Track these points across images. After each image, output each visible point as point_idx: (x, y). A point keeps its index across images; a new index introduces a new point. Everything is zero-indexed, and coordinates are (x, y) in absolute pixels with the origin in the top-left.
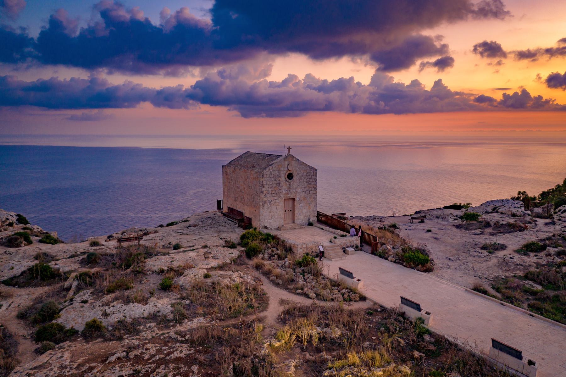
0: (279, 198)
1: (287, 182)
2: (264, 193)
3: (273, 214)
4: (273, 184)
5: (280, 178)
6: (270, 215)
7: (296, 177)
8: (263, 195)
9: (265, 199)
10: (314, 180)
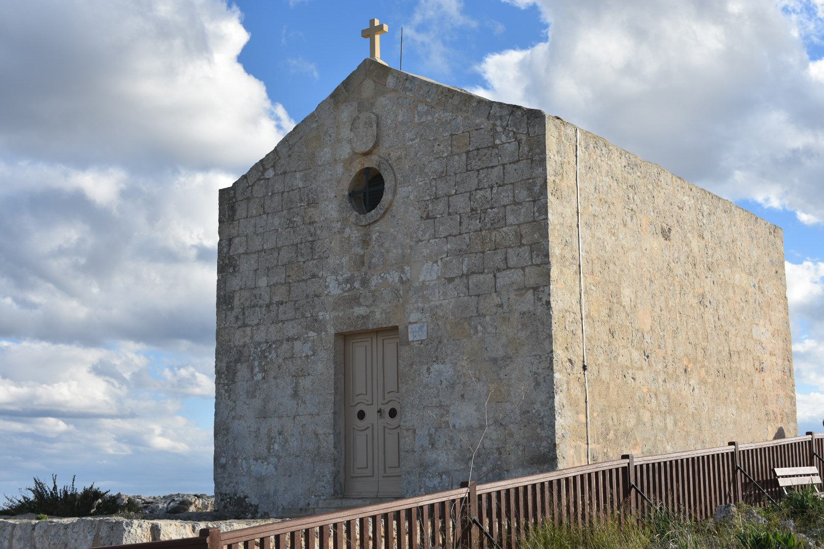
0: (308, 328)
2: (236, 302)
3: (275, 424)
4: (279, 249)
5: (311, 211)
6: (264, 431)
8: (231, 317)
9: (239, 338)
10: (523, 195)
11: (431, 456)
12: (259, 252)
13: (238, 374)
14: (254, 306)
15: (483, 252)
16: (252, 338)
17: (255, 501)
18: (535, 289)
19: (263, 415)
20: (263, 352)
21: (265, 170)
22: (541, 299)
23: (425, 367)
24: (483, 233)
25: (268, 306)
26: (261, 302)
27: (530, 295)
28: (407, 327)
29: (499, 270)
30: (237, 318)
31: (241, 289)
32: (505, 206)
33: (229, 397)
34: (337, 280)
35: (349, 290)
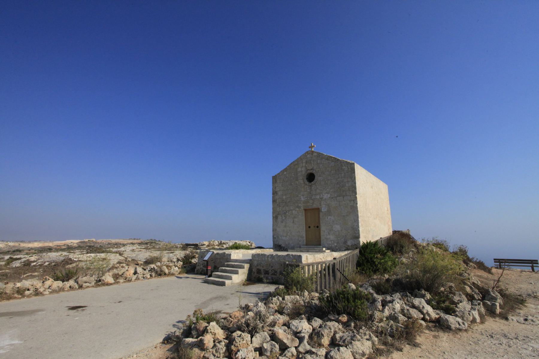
1: (306, 186)
2: (277, 201)
7: (320, 178)
9: (278, 209)
11: (328, 237)
12: (283, 190)
13: (279, 218)
14: (282, 202)
15: (340, 192)
16: (282, 209)
17: (283, 246)
18: (354, 201)
19: (285, 226)
20: (285, 213)
21: (284, 172)
22: (355, 203)
23: (326, 217)
24: (340, 188)
25: (286, 202)
26: (284, 201)
27: (352, 202)
28: (321, 208)
29: (344, 196)
30: (278, 205)
31: (279, 199)
32: (345, 182)
33: (276, 223)
34: (303, 197)
35: (306, 200)
